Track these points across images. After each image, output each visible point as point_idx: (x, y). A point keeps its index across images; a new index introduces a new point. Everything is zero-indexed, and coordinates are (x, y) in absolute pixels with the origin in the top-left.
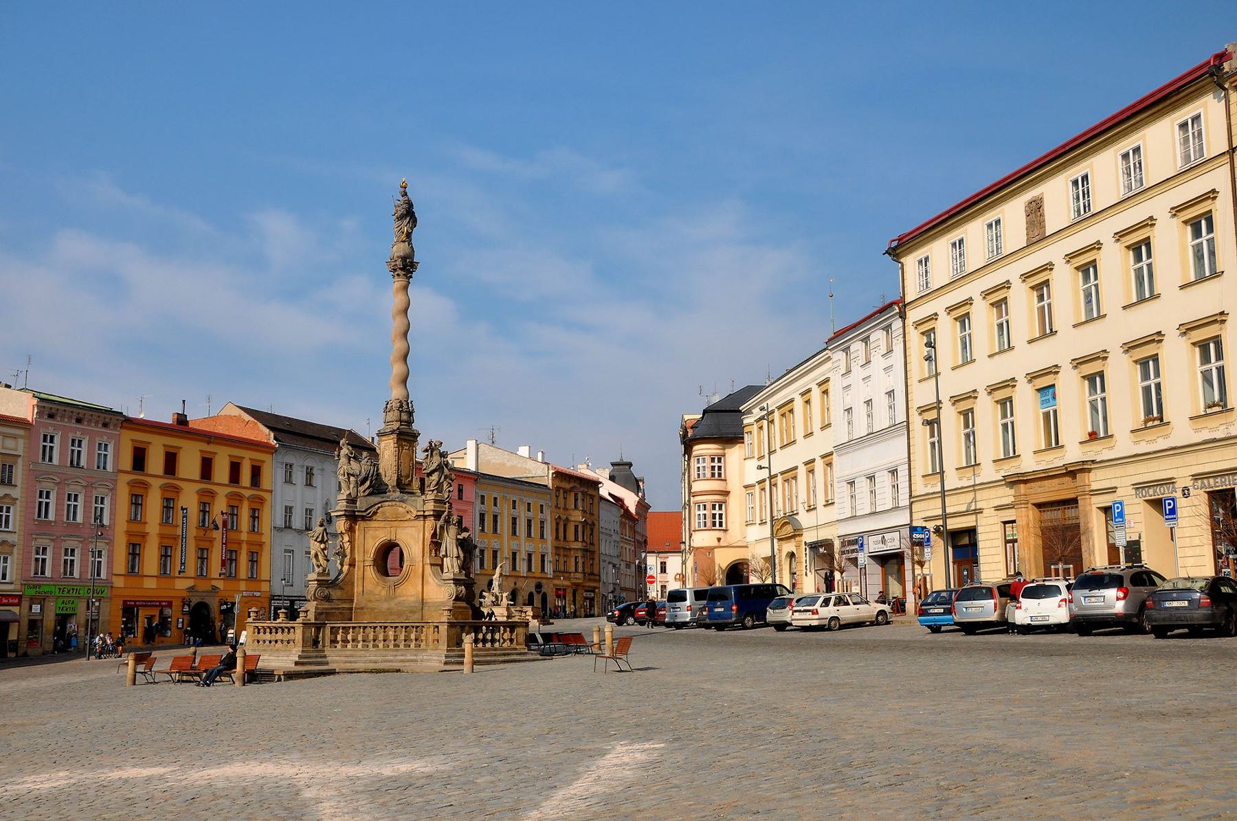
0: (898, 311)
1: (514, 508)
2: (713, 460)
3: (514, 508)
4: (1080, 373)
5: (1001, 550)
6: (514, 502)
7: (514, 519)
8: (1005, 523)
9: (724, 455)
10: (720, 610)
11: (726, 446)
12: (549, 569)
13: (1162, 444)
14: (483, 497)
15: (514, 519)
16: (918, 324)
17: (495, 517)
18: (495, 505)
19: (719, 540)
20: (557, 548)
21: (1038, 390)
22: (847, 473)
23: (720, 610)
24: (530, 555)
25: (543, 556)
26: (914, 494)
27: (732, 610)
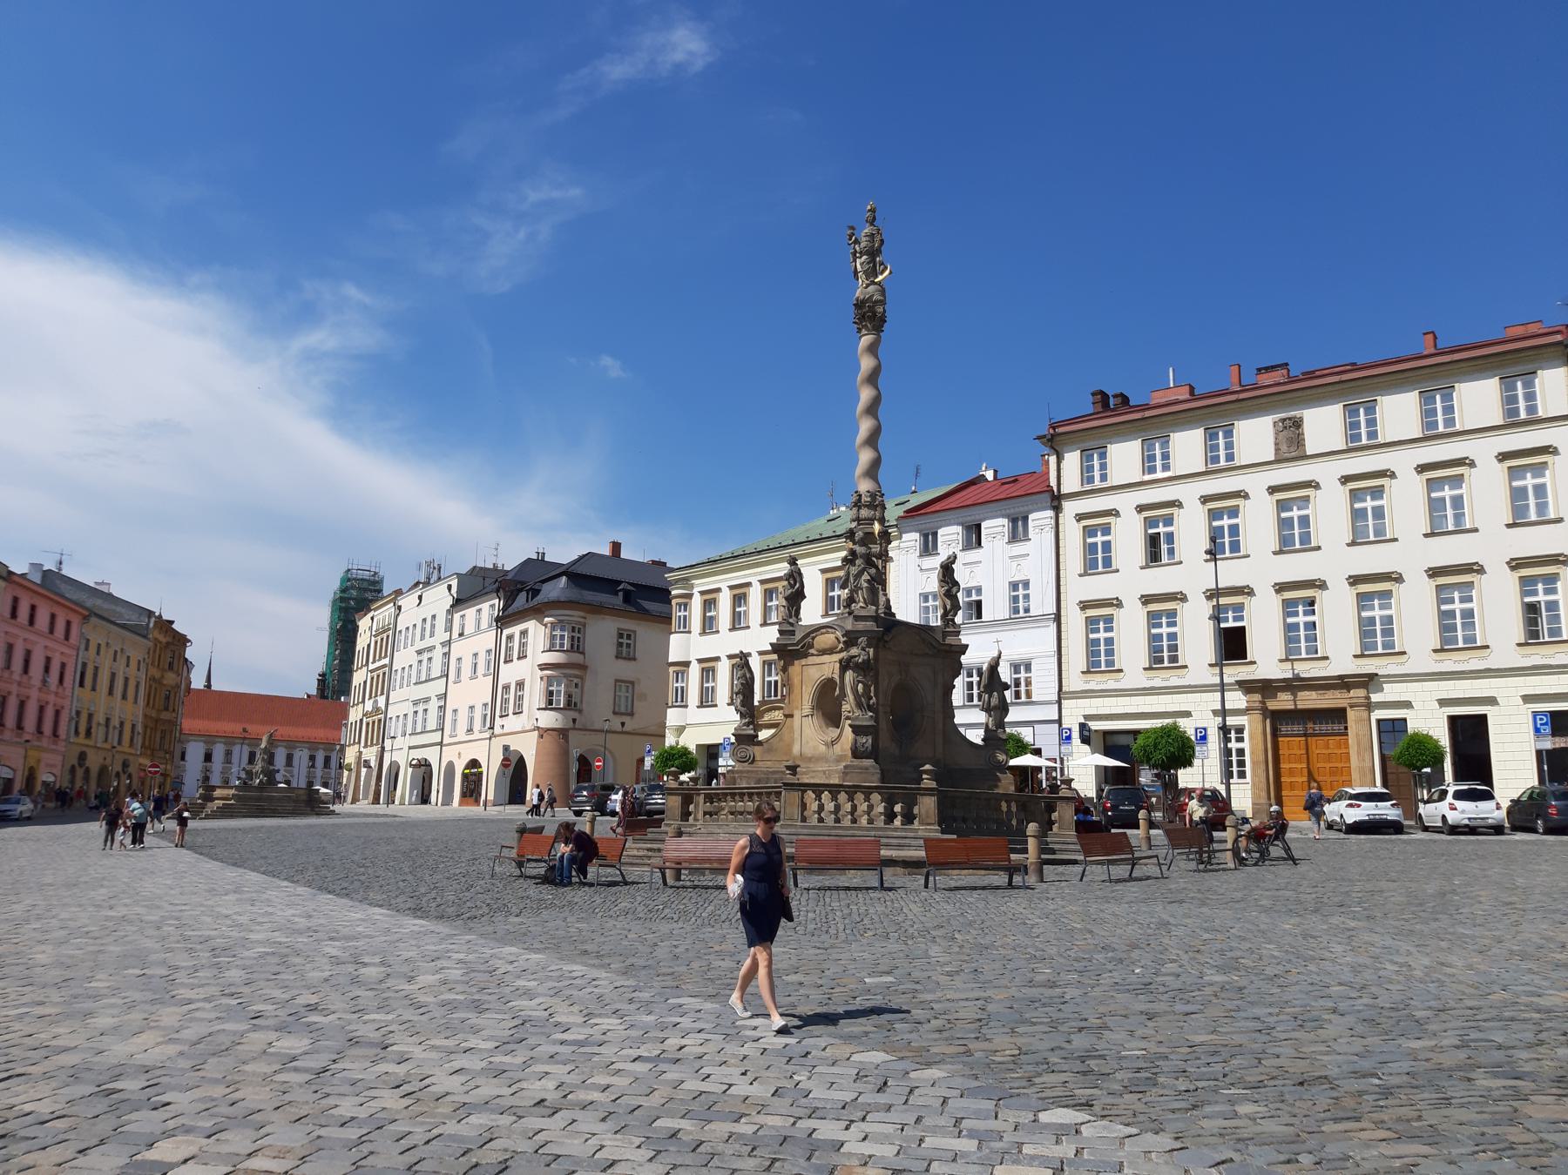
1: (115, 660)
2: (573, 630)
3: (115, 660)
6: (116, 652)
7: (113, 675)
9: (584, 626)
11: (588, 615)
12: (139, 740)
14: (88, 640)
15: (113, 675)
16: (1080, 517)
17: (96, 668)
18: (98, 653)
19: (574, 721)
20: (145, 716)
24: (122, 724)
25: (133, 726)
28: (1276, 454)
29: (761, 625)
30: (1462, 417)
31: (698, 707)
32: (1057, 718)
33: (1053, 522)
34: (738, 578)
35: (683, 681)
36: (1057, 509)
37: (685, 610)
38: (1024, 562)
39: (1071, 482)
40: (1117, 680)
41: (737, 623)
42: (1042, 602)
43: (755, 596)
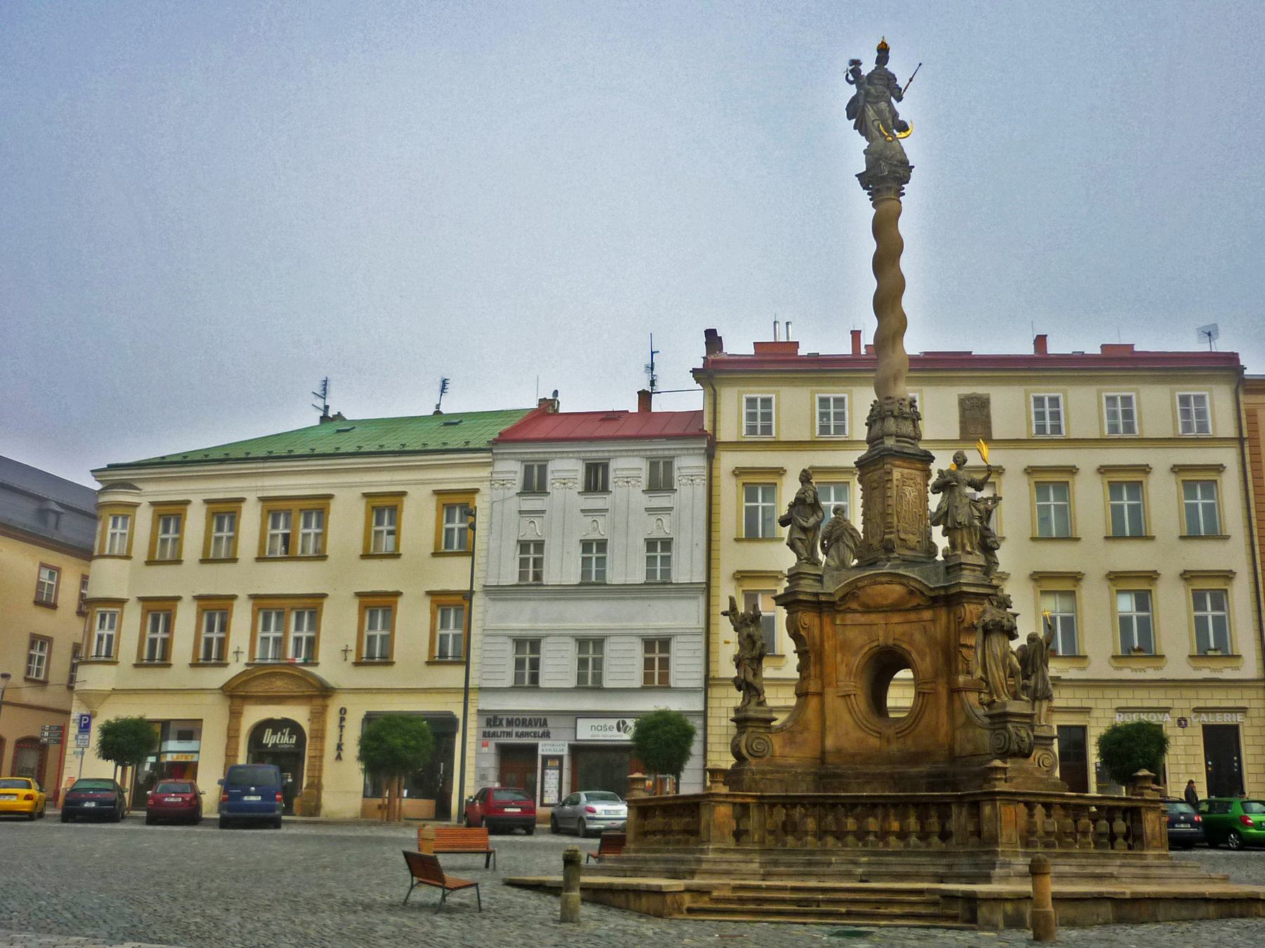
0: (705, 446)
4: (1040, 587)
10: (253, 798)
13: (1151, 674)
16: (739, 472)
22: (526, 625)
23: (253, 798)
26: (711, 675)
27: (276, 800)
31: (136, 666)
32: (700, 708)
33: (705, 472)
34: (223, 489)
35: (111, 627)
36: (710, 456)
37: (124, 526)
38: (666, 519)
39: (731, 426)
40: (778, 668)
42: (687, 568)
43: (250, 520)
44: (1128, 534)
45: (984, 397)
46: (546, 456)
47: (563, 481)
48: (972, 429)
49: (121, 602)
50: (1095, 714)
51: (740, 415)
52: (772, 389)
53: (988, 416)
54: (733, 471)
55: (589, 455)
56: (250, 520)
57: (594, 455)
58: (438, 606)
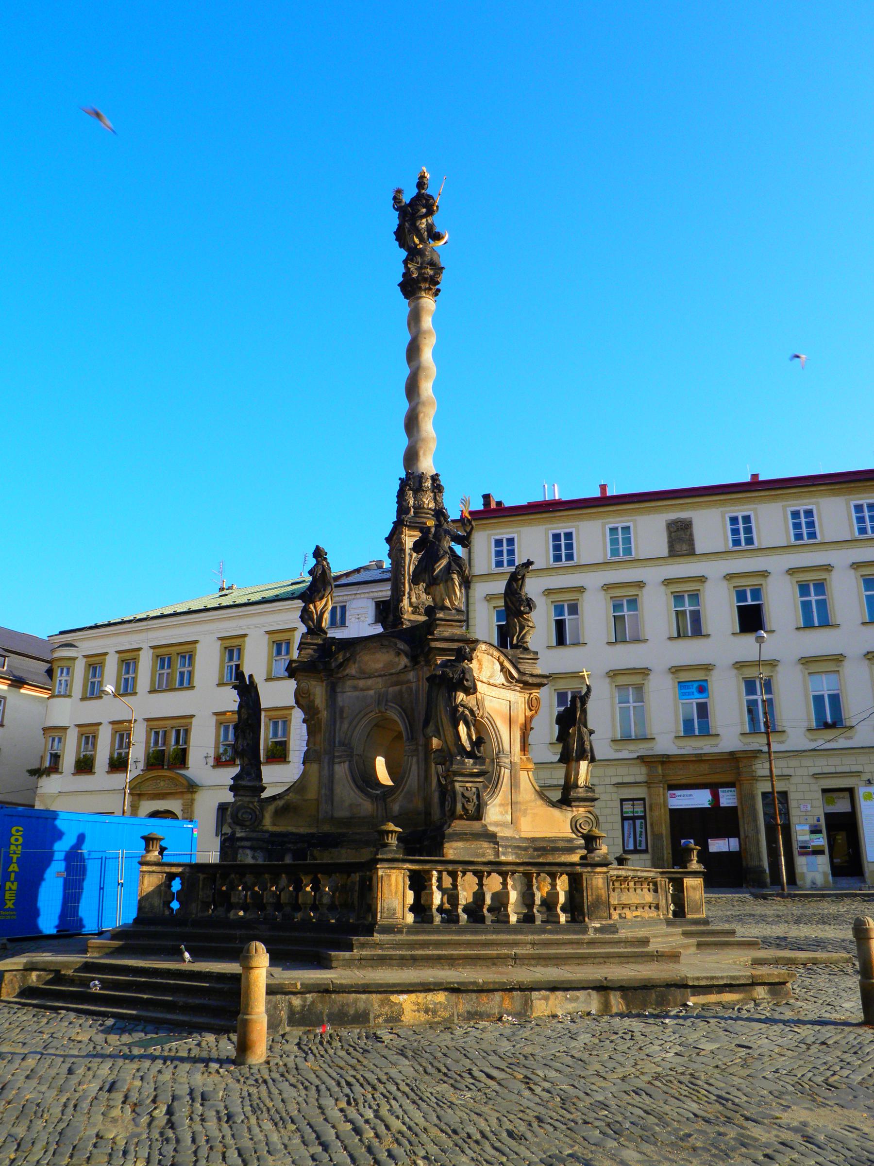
4: (742, 674)
5: (618, 826)
8: (622, 800)
13: (842, 743)
21: (679, 682)
28: (670, 551)
29: (150, 692)
30: (822, 531)
41: (126, 689)
44: (816, 624)
45: (688, 520)
46: (345, 598)
47: (357, 617)
48: (677, 547)
49: (65, 729)
50: (793, 780)
51: (490, 552)
52: (514, 530)
53: (691, 535)
54: (485, 598)
55: (375, 594)
56: (145, 663)
57: (380, 594)
58: (270, 719)
